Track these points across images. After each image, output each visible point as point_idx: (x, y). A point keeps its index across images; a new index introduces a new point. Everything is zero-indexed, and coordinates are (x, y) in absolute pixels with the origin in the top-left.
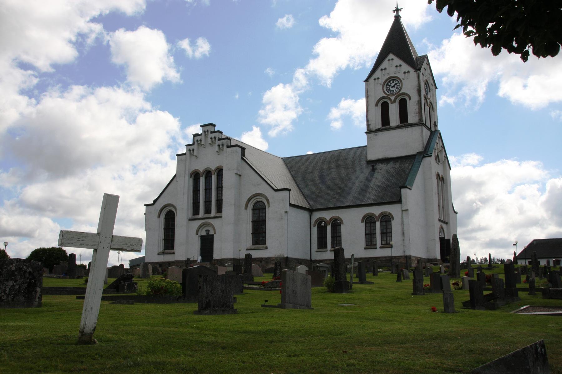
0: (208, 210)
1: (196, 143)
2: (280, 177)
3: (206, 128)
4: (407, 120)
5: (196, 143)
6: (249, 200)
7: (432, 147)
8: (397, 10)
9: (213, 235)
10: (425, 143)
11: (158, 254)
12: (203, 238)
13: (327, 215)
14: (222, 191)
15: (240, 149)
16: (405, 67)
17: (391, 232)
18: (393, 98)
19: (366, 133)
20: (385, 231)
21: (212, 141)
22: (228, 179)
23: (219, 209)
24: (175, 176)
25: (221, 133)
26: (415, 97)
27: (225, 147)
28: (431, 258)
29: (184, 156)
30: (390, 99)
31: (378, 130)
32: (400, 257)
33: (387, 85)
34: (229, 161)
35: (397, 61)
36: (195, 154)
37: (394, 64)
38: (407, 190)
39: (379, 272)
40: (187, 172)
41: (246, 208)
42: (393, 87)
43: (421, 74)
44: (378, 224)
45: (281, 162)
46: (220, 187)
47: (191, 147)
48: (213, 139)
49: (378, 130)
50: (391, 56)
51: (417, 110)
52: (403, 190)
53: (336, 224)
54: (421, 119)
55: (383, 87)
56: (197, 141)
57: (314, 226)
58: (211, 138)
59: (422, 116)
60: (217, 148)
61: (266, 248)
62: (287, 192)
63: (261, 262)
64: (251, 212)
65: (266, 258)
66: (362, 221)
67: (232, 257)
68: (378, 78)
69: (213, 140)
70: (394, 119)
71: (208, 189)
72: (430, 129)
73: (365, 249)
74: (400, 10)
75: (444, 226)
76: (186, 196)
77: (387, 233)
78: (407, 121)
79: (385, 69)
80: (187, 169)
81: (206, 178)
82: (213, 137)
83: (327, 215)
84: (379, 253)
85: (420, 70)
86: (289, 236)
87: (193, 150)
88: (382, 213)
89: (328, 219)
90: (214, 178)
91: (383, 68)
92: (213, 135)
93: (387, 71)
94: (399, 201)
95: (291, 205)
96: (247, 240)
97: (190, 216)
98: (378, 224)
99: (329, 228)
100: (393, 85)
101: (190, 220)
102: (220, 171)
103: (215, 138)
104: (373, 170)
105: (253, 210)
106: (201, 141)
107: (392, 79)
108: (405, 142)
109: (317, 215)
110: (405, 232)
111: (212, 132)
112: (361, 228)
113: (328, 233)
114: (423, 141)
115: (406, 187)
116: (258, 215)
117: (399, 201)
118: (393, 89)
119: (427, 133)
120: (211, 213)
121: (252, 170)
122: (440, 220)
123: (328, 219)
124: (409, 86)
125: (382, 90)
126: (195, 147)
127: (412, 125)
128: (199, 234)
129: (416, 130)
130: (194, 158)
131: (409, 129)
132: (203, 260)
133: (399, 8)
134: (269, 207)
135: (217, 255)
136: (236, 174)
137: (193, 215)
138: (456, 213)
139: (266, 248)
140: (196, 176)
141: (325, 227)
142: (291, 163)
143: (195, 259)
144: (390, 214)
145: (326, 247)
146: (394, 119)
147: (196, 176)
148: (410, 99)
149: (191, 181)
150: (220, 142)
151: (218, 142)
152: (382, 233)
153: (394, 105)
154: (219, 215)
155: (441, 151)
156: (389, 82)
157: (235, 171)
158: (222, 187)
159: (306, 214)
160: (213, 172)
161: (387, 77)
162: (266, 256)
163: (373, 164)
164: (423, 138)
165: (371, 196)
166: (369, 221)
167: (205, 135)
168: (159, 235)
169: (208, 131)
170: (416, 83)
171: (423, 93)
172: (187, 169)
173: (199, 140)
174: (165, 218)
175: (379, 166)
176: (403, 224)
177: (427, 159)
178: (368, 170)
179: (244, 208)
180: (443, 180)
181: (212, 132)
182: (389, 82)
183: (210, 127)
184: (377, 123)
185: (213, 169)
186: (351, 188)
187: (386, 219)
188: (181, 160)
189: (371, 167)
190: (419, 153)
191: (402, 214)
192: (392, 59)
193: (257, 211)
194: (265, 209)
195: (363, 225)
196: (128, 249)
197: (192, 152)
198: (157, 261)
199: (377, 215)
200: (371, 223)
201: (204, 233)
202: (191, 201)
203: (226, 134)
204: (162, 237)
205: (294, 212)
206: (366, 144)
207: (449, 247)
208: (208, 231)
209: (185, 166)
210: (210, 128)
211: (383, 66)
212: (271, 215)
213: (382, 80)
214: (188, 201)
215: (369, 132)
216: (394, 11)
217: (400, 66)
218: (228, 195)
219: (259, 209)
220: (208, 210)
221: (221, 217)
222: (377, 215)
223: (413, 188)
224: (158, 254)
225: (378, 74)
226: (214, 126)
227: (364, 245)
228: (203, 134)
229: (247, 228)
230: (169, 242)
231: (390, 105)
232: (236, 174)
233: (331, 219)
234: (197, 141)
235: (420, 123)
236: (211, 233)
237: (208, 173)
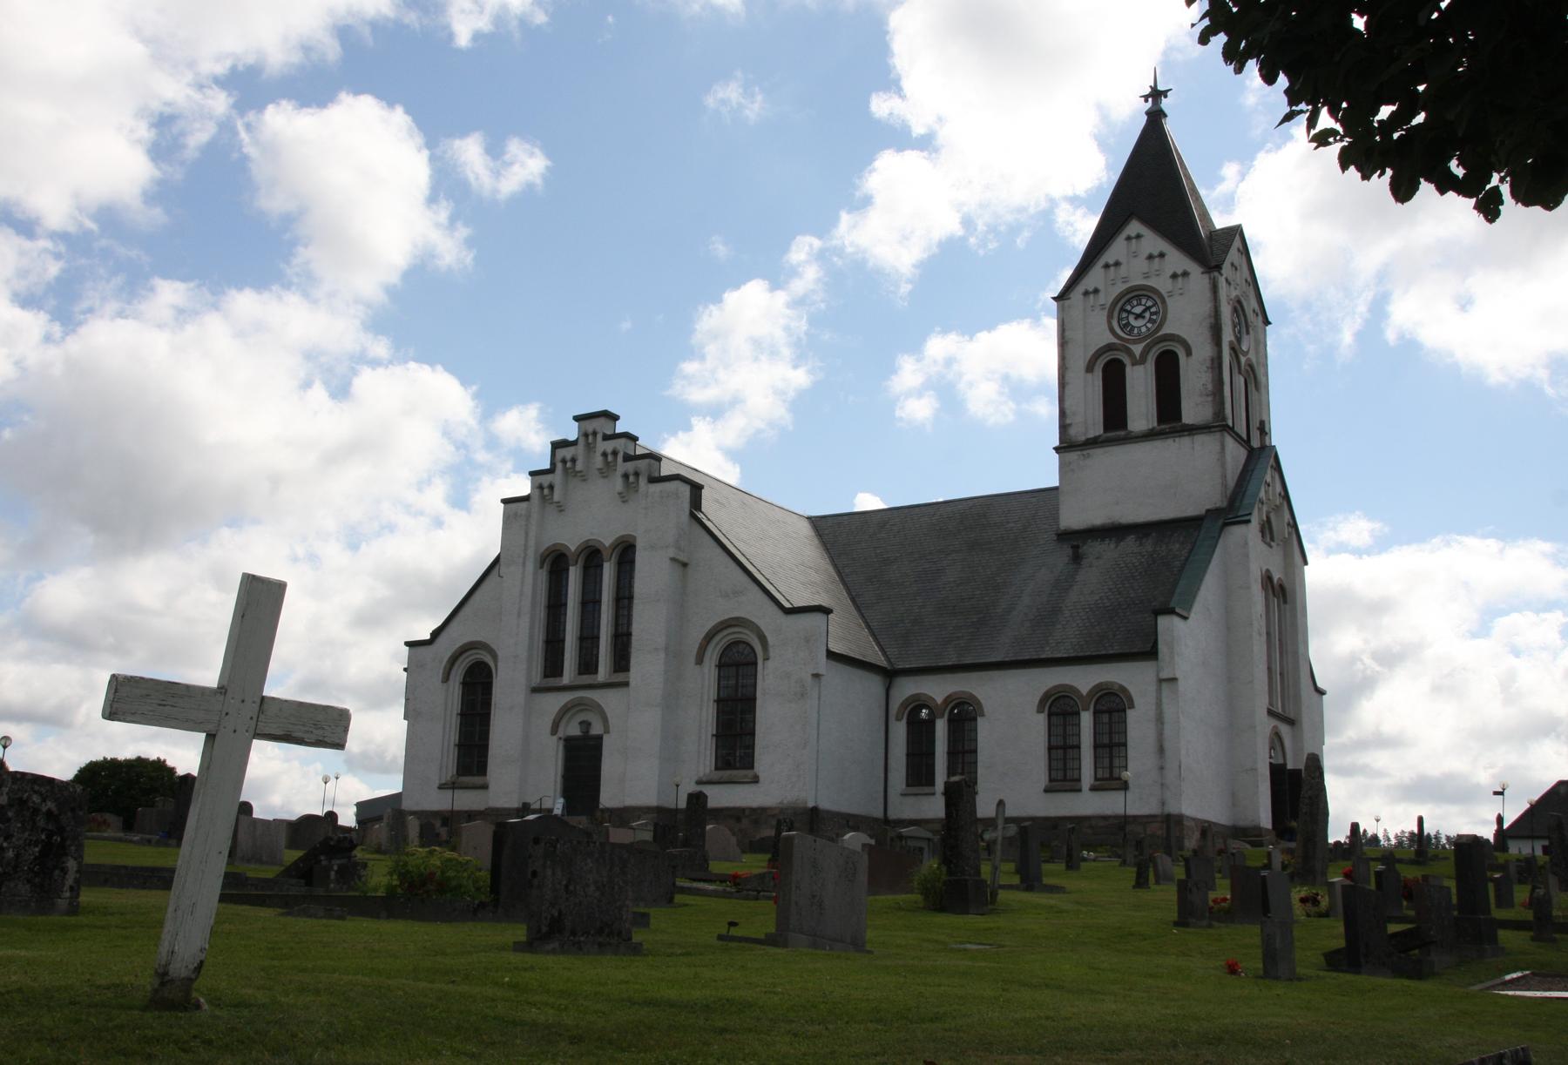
0: (588, 664)
1: (559, 466)
2: (798, 573)
3: (591, 426)
5: (559, 466)
6: (709, 637)
7: (1253, 497)
8: (1156, 94)
9: (600, 738)
10: (1231, 483)
11: (441, 787)
13: (938, 689)
14: (630, 608)
15: (686, 490)
16: (1176, 260)
17: (1125, 745)
18: (1137, 349)
19: (1056, 449)
20: (1106, 740)
21: (607, 463)
22: (651, 574)
23: (622, 661)
24: (497, 560)
25: (634, 439)
26: (1202, 349)
27: (643, 481)
28: (1242, 823)
29: (524, 505)
30: (1129, 352)
31: (1093, 443)
33: (1122, 310)
34: (652, 524)
35: (1152, 242)
36: (556, 497)
37: (1142, 245)
38: (1176, 620)
39: (1085, 860)
40: (531, 552)
41: (700, 660)
42: (1138, 316)
43: (1222, 281)
44: (1086, 719)
45: (806, 529)
46: (624, 599)
47: (546, 480)
48: (610, 458)
49: (1093, 443)
50: (1134, 227)
51: (1210, 387)
52: (1163, 621)
53: (964, 715)
54: (1219, 413)
55: (1110, 317)
56: (564, 461)
57: (898, 719)
58: (605, 454)
59: (1222, 403)
60: (618, 484)
61: (755, 780)
62: (818, 618)
63: (738, 819)
64: (714, 672)
65: (753, 810)
66: (1040, 710)
67: (652, 801)
68: (1096, 291)
69: (609, 460)
70: (1141, 408)
71: (590, 603)
72: (1246, 442)
73: (1046, 791)
74: (1165, 93)
75: (1284, 729)
76: (525, 622)
77: (1112, 746)
78: (1180, 418)
79: (1117, 264)
81: (586, 568)
82: (609, 450)
83: (938, 689)
84: (1088, 804)
85: (1218, 268)
86: (820, 747)
87: (551, 487)
88: (1100, 684)
89: (939, 700)
90: (608, 572)
91: (1111, 262)
92: (609, 446)
93: (1123, 270)
94: (1151, 653)
95: (831, 655)
96: (699, 756)
97: (537, 679)
98: (1086, 719)
99: (941, 727)
100: (1138, 310)
101: (536, 690)
102: (626, 552)
103: (615, 453)
104: (1077, 558)
105: (720, 666)
106: (574, 460)
107: (1136, 293)
108: (1167, 478)
109: (907, 688)
110: (1167, 745)
111: (606, 438)
113: (938, 742)
114: (1224, 476)
115: (1172, 612)
116: (732, 682)
117: (1150, 653)
118: (1140, 323)
119: (1235, 454)
120: (596, 672)
121: (719, 550)
122: (1271, 713)
123: (939, 700)
124: (1186, 314)
125: (1106, 326)
126: (557, 478)
127: (1192, 430)
128: (561, 733)
129: (1205, 445)
131: (1185, 441)
132: (568, 808)
133: (1161, 88)
134: (766, 659)
135: (610, 796)
136: (673, 560)
137: (546, 676)
138: (1321, 693)
139: (755, 780)
140: (556, 562)
141: (930, 723)
142: (834, 532)
143: (547, 804)
144: (1124, 689)
145: (931, 782)
146: (1141, 408)
147: (556, 562)
148: (1189, 353)
149: (543, 575)
150: (630, 466)
151: (622, 467)
152: (1096, 747)
153: (1140, 368)
154: (620, 677)
155: (1277, 509)
156: (1129, 301)
157: (671, 553)
158: (631, 598)
159: (875, 684)
160: (605, 554)
161: (1121, 287)
162: (755, 805)
163: (1077, 540)
164: (1223, 465)
165: (1066, 638)
166: (1059, 707)
167: (588, 445)
168: (445, 732)
169: (595, 434)
170: (1207, 307)
171: (1228, 336)
172: (532, 543)
173: (568, 457)
174: (464, 684)
175: (1093, 549)
176: (1160, 719)
177: (1237, 530)
178: (1062, 557)
179: (692, 659)
180: (1283, 594)
181: (606, 438)
182: (1129, 301)
183: (602, 420)
184: (1091, 421)
187: (1112, 704)
189: (1070, 551)
190: (1213, 513)
191: (1159, 691)
192: (1138, 236)
194: (755, 664)
195: (1042, 719)
196: (307, 737)
197: (546, 491)
198: (436, 807)
199: (1084, 691)
200: (1065, 714)
201: (574, 730)
202: (540, 637)
203: (646, 443)
204: (454, 737)
205: (838, 677)
206: (1055, 482)
207: (1299, 790)
208: (586, 725)
209: (527, 534)
210: (601, 426)
211: (1110, 256)
212: (771, 681)
213: (1107, 297)
214: (531, 637)
215: (1066, 446)
216: (1146, 98)
217: (1162, 255)
218: (648, 622)
219: (738, 665)
220: (588, 664)
221: (626, 684)
222: (1084, 691)
223: (1192, 615)
224: (441, 787)
225: (1095, 277)
226: (615, 418)
227: (1042, 778)
229: (701, 718)
230: (472, 752)
231: (1128, 369)
232: (673, 560)
233: (947, 700)
234: (564, 461)
235: (1218, 425)
236: (596, 730)
237: (592, 556)
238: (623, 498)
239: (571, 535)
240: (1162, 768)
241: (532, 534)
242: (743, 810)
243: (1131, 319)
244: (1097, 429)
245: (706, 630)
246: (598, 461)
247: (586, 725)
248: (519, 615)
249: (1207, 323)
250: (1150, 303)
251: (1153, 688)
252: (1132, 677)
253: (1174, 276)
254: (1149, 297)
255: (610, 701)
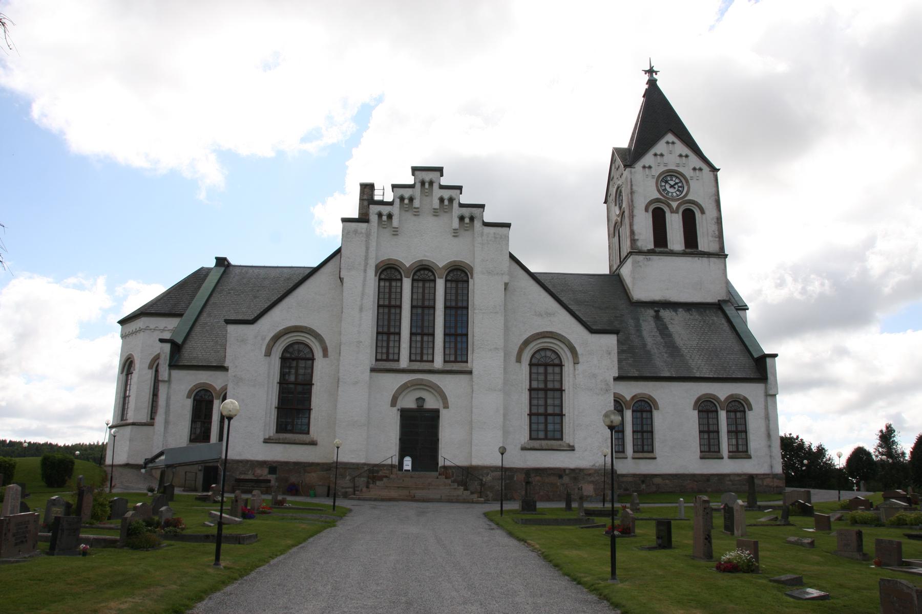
0: (421, 353)
3: (428, 176)
4: (665, 244)
6: (526, 343)
8: (651, 71)
12: (407, 417)
18: (674, 205)
22: (484, 293)
27: (477, 224)
30: (669, 206)
31: (650, 252)
32: (764, 476)
35: (681, 148)
40: (372, 264)
41: (519, 360)
42: (672, 186)
51: (717, 233)
58: (442, 200)
60: (456, 223)
61: (572, 448)
63: (560, 477)
65: (573, 470)
67: (494, 460)
68: (650, 167)
71: (423, 308)
74: (656, 72)
77: (739, 431)
78: (696, 246)
80: (372, 255)
84: (726, 466)
87: (390, 216)
93: (665, 159)
100: (672, 183)
102: (459, 275)
105: (531, 365)
106: (411, 199)
112: (692, 418)
118: (672, 190)
124: (697, 192)
125: (655, 188)
130: (386, 233)
134: (576, 362)
139: (572, 448)
140: (389, 272)
147: (389, 272)
157: (506, 279)
169: (431, 183)
174: (283, 359)
179: (513, 358)
185: (441, 265)
186: (645, 345)
187: (738, 407)
188: (356, 232)
191: (766, 402)
193: (541, 370)
198: (260, 457)
199: (722, 398)
201: (409, 402)
204: (275, 402)
208: (420, 400)
209: (367, 249)
213: (656, 171)
216: (646, 72)
219: (546, 365)
220: (421, 353)
222: (722, 398)
224: (266, 441)
228: (418, 185)
231: (668, 215)
233: (633, 398)
236: (431, 403)
237: (423, 273)
238: (456, 233)
239: (407, 253)
240: (770, 446)
241: (373, 248)
242: (564, 470)
243: (667, 187)
244: (651, 246)
245: (525, 337)
246: (436, 203)
247: (420, 400)
248: (361, 310)
249: (713, 198)
250: (677, 181)
251: (762, 399)
252: (750, 391)
253: (694, 169)
254: (677, 177)
255: (448, 383)
